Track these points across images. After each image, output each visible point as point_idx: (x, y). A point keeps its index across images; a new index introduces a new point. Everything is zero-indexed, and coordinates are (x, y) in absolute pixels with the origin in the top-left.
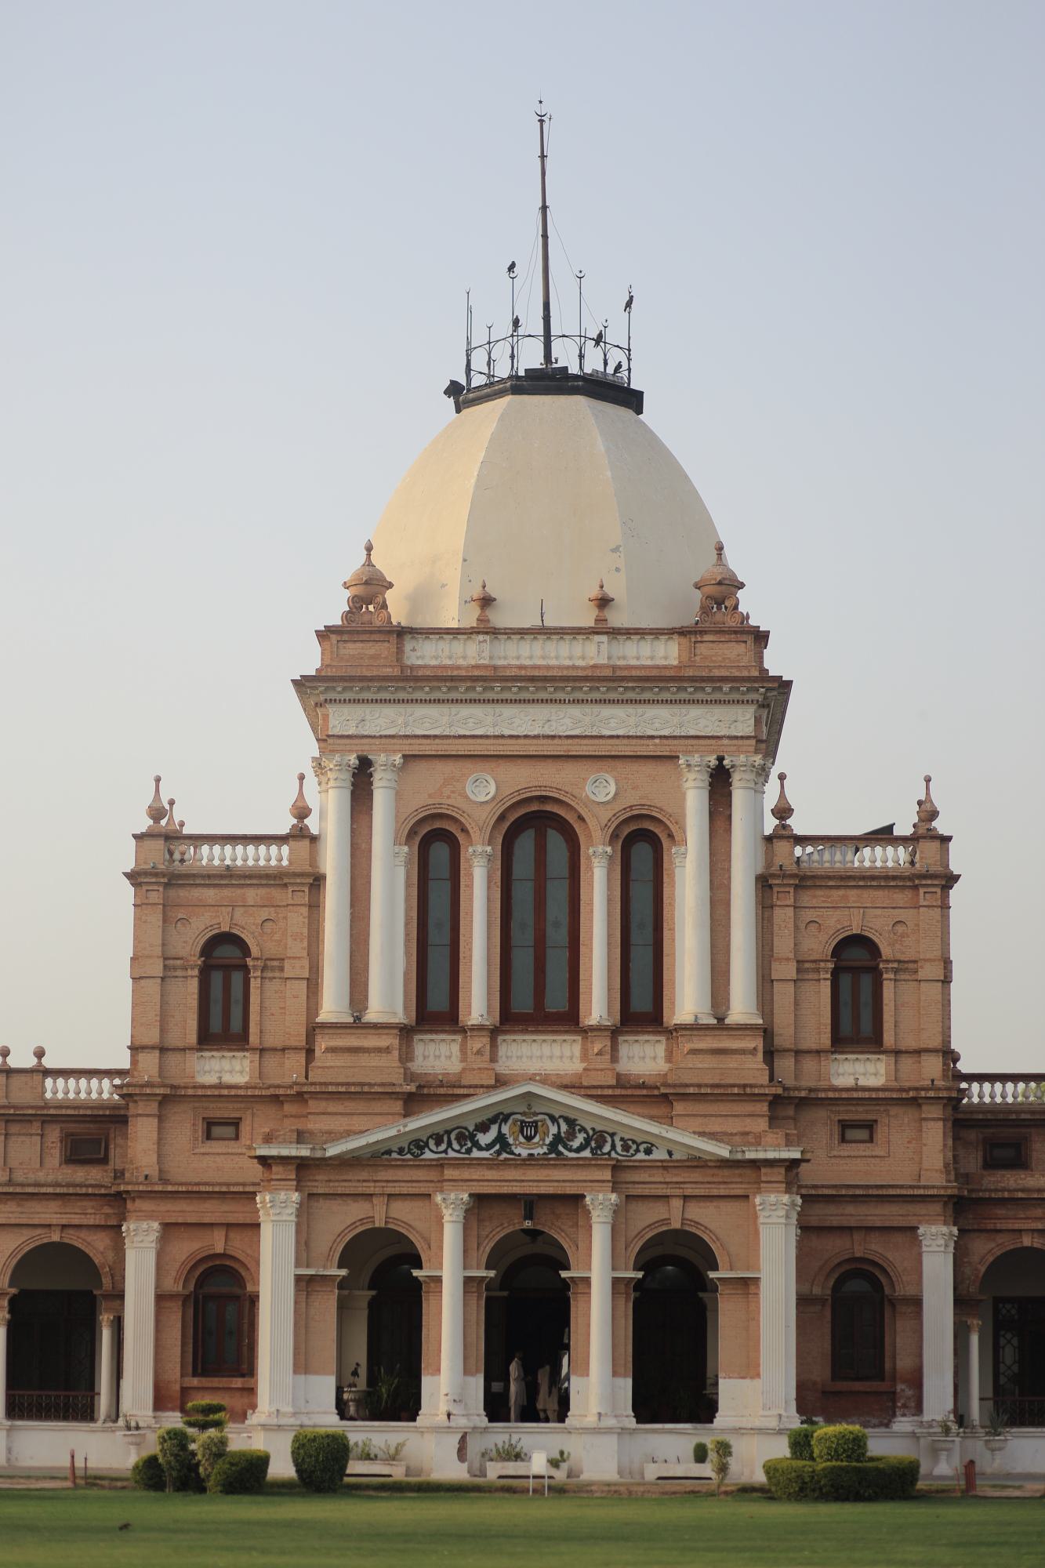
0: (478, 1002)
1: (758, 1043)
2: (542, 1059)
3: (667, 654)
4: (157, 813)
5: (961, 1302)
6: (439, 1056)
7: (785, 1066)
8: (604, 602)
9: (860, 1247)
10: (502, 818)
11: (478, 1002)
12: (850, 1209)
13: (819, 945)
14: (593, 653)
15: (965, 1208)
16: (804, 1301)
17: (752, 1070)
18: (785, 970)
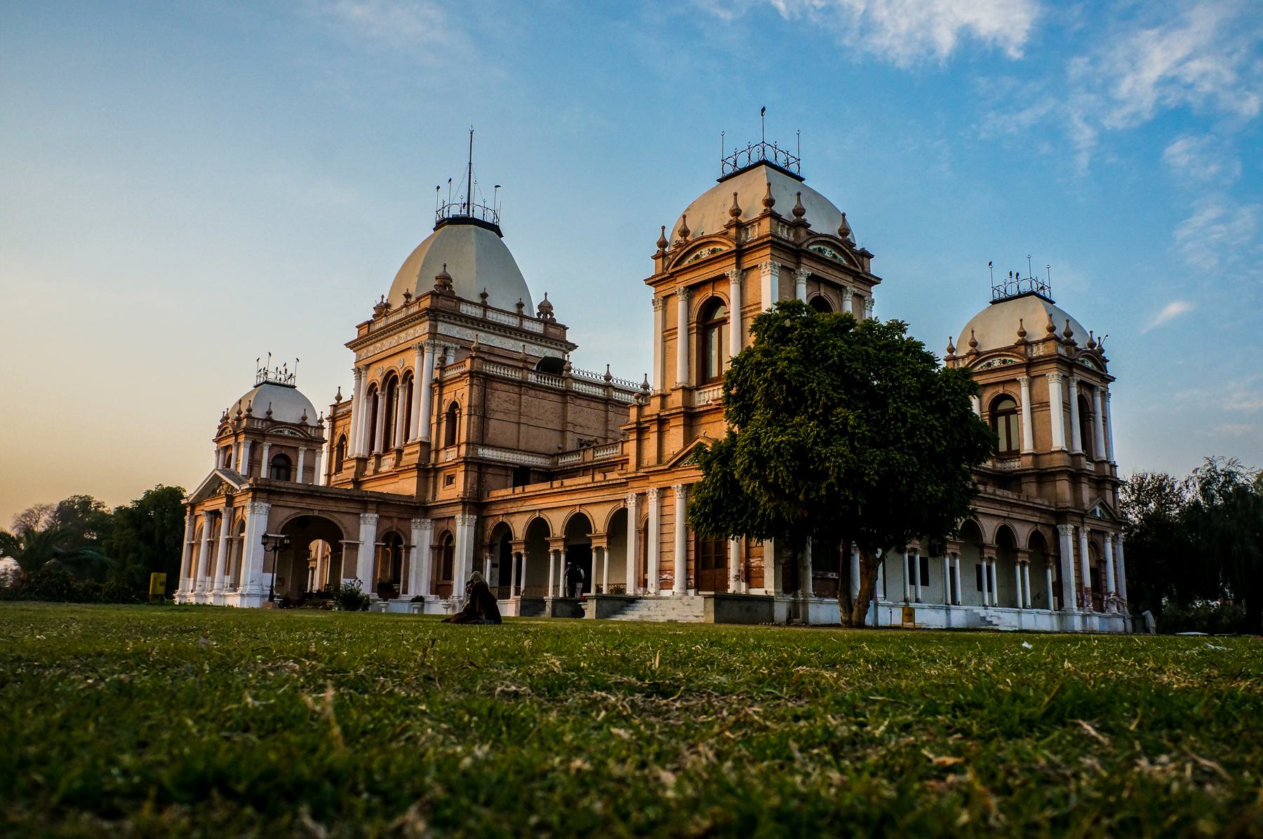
0: (378, 448)
1: (418, 448)
2: (388, 463)
3: (415, 309)
4: (339, 398)
5: (479, 547)
6: (371, 466)
7: (433, 455)
8: (408, 296)
9: (443, 525)
10: (385, 379)
11: (378, 448)
12: (443, 510)
13: (445, 408)
14: (402, 315)
15: (476, 504)
16: (432, 547)
17: (415, 459)
18: (434, 420)
